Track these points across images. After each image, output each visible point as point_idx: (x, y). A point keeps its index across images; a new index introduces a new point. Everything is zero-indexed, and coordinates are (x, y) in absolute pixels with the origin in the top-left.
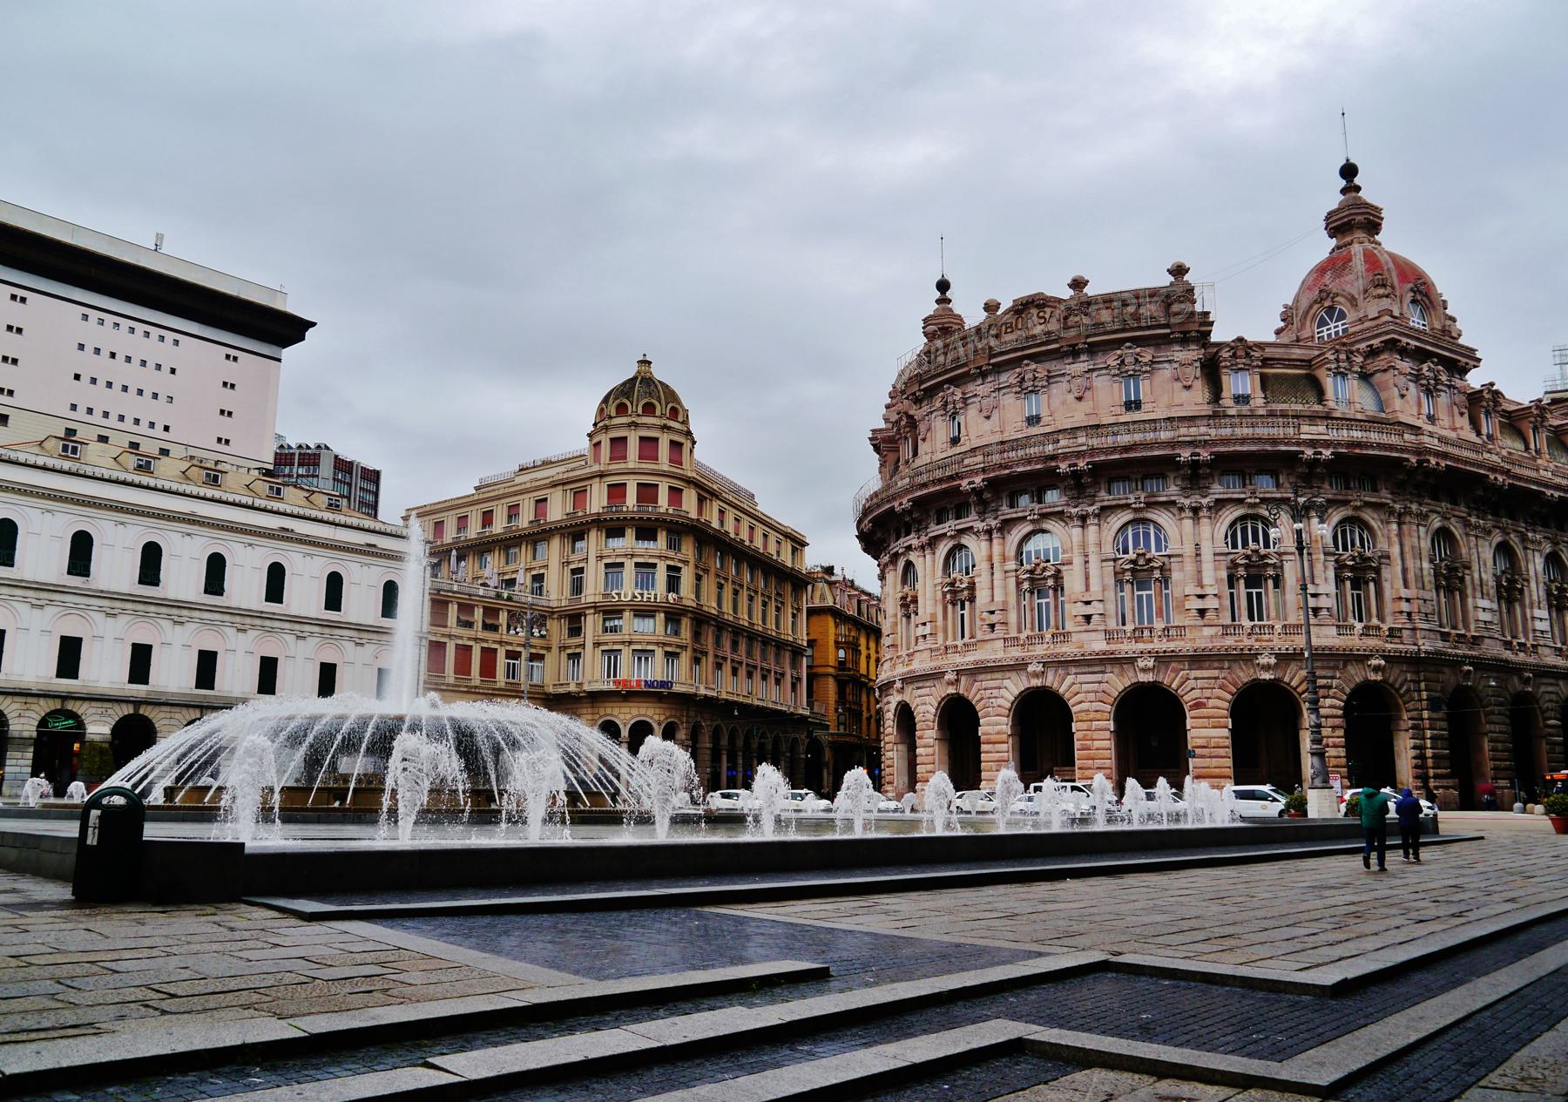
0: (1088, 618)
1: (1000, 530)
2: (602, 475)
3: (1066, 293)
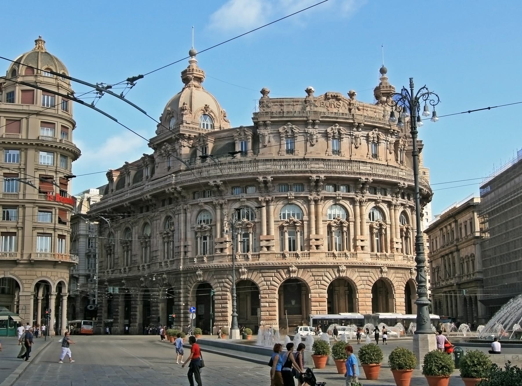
0: (362, 247)
2: (38, 114)
3: (349, 97)
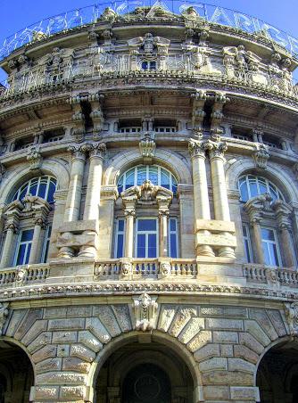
1: (101, 150)
